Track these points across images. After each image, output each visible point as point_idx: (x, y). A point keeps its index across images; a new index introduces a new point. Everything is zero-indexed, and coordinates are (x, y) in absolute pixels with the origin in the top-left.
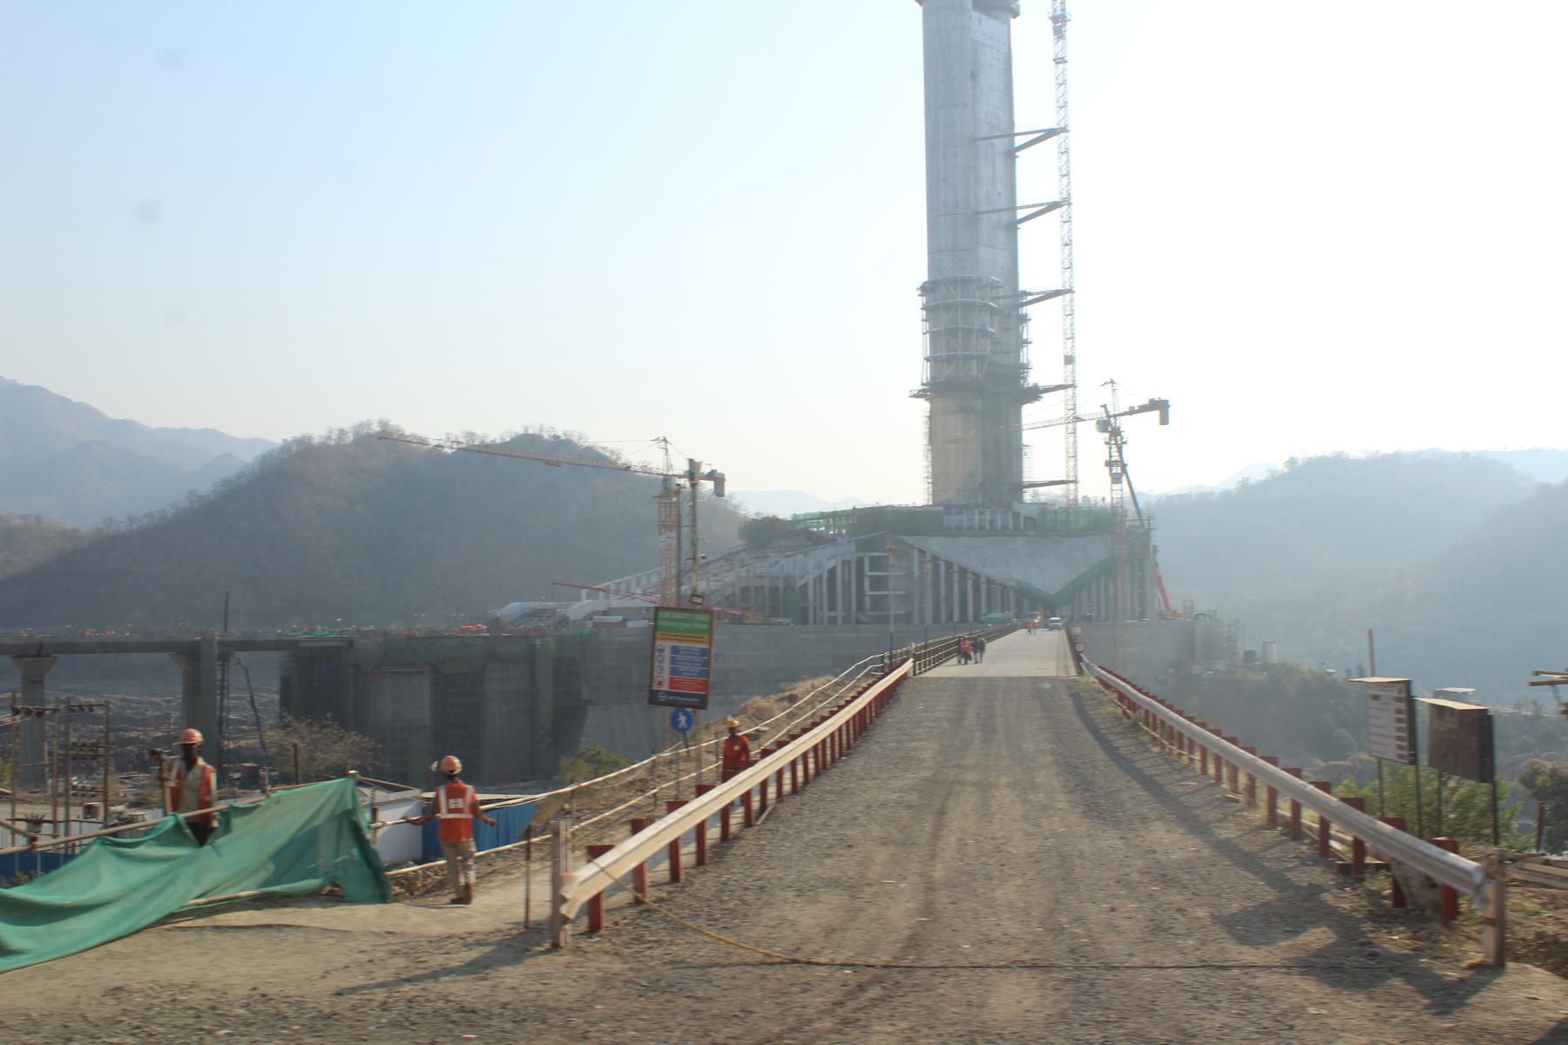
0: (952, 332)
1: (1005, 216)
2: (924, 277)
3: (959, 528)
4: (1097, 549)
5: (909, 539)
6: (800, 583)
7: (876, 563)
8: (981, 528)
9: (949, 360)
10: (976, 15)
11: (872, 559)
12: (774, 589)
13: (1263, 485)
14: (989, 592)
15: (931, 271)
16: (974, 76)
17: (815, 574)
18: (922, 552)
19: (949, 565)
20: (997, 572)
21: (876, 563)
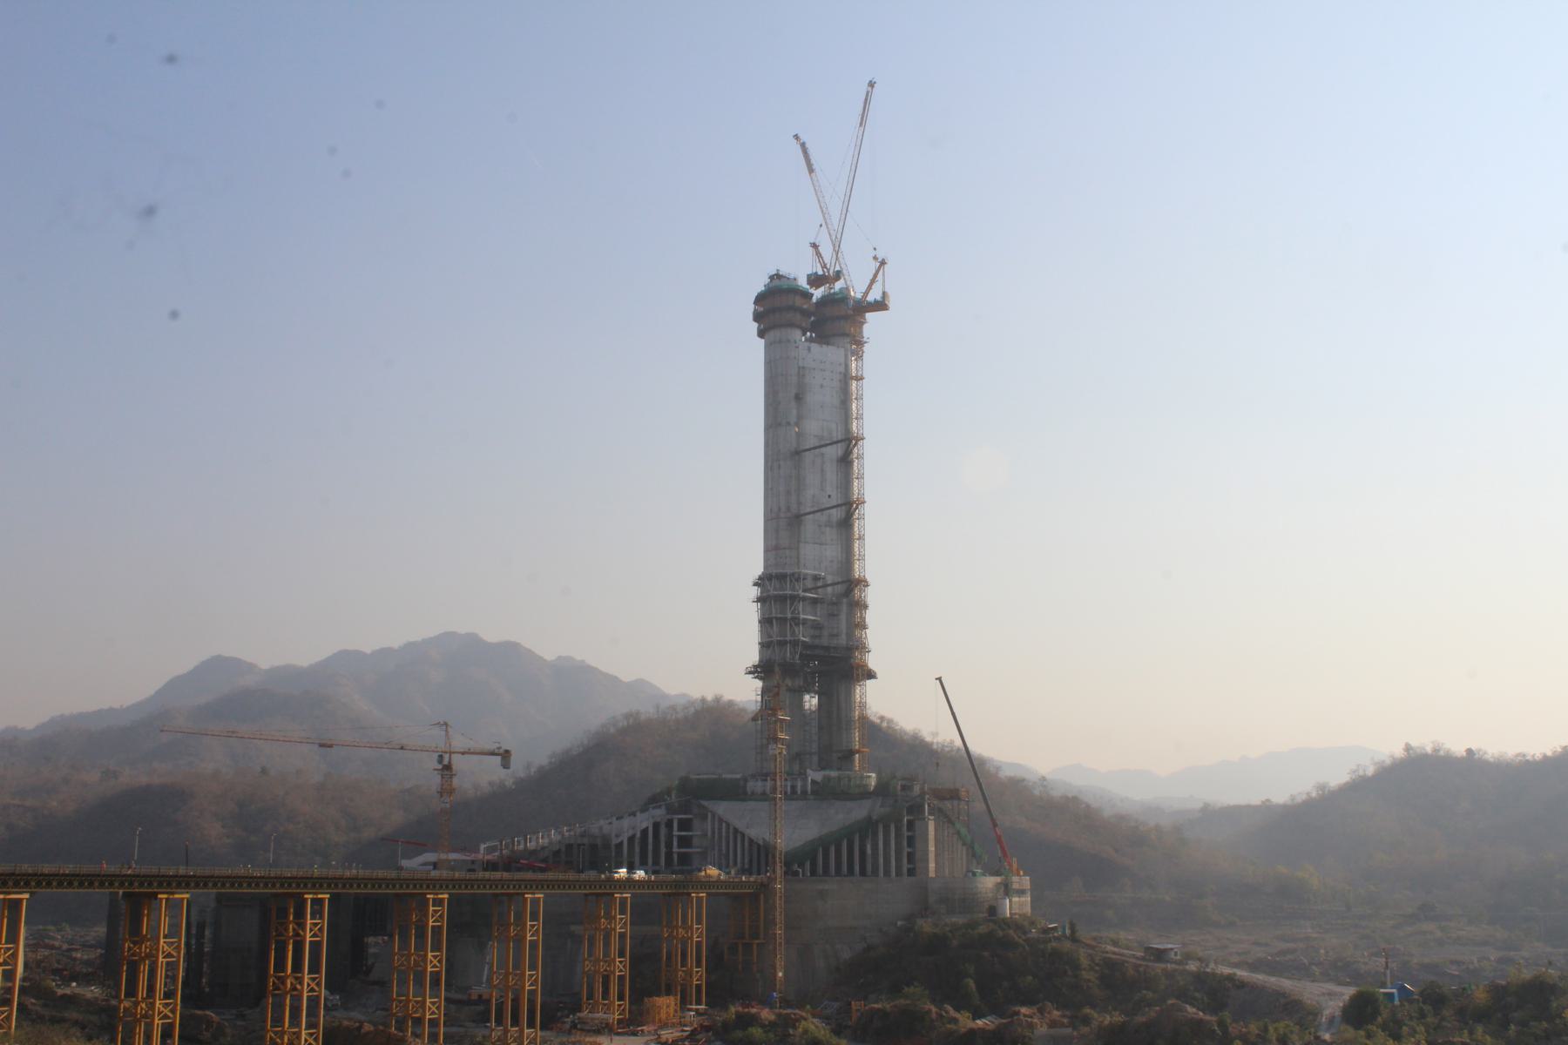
1: (837, 514)
2: (758, 569)
4: (858, 812)
5: (705, 803)
6: (615, 841)
11: (680, 821)
12: (594, 847)
16: (799, 398)
17: (631, 833)
19: (728, 825)
20: (753, 833)
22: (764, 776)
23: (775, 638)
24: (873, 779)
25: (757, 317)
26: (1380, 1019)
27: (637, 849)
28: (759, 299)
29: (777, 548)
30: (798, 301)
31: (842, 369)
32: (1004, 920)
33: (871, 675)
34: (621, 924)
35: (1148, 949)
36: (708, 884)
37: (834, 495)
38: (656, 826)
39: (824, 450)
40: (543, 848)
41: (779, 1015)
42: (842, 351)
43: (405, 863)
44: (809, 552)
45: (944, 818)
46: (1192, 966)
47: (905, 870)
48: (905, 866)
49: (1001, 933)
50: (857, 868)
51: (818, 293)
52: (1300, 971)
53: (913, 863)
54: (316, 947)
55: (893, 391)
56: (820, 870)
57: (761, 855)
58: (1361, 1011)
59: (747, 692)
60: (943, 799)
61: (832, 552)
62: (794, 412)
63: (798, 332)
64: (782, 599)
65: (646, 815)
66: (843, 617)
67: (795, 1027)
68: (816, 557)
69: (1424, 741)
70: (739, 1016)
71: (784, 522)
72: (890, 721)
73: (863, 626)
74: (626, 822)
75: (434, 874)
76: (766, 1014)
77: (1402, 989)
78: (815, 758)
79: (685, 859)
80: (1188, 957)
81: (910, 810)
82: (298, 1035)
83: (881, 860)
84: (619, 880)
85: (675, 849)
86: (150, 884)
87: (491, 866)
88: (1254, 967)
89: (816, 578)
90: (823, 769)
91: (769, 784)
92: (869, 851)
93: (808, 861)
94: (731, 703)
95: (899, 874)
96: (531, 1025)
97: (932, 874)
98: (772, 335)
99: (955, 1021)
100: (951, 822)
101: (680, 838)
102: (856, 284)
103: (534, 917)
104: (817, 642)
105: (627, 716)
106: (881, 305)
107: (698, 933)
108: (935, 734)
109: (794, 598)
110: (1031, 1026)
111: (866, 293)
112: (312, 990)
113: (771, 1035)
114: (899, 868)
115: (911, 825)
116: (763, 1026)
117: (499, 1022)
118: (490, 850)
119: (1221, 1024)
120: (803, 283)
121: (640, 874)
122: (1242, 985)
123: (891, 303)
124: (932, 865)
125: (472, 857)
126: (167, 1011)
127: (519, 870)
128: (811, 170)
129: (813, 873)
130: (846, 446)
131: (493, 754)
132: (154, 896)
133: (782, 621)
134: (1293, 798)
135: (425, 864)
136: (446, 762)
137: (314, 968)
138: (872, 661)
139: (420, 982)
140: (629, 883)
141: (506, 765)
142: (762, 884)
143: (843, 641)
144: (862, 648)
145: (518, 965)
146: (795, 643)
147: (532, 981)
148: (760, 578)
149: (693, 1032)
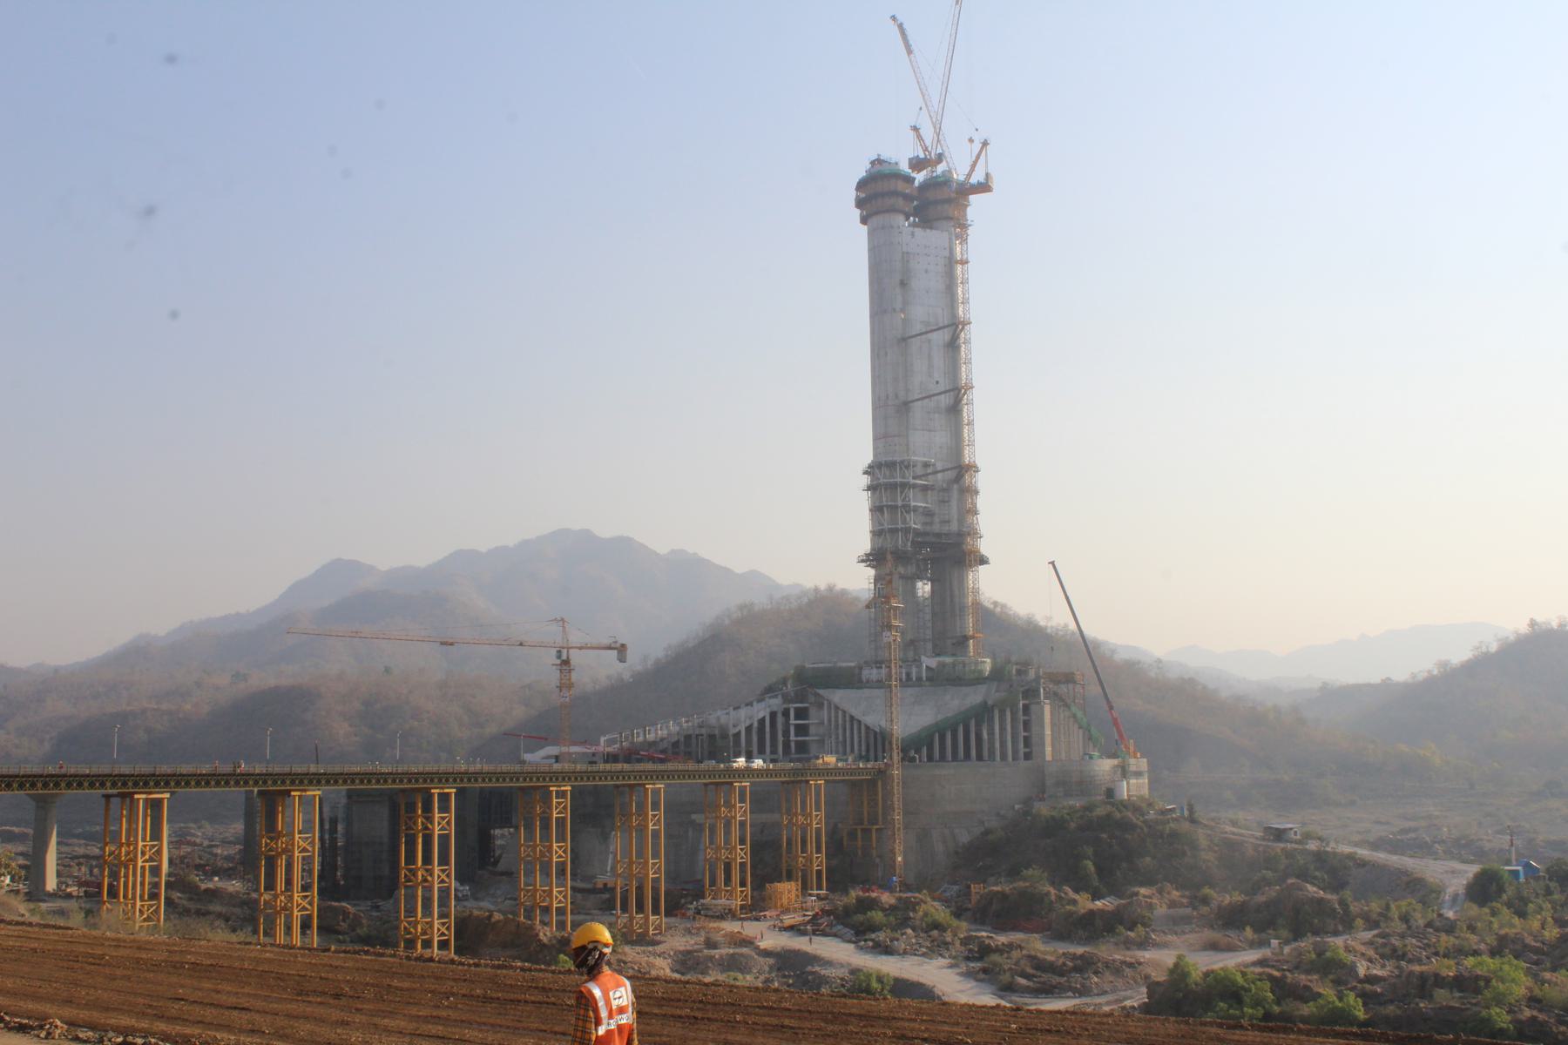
1: (945, 400)
2: (868, 458)
4: (974, 697)
5: (821, 692)
6: (733, 731)
12: (712, 737)
14: (867, 737)
15: (875, 455)
16: (903, 284)
21: (802, 713)
22: (878, 664)
23: (886, 526)
24: (987, 665)
25: (860, 204)
26: (1505, 897)
27: (755, 738)
28: (861, 185)
30: (901, 186)
31: (947, 253)
32: (1122, 802)
33: (983, 561)
34: (741, 812)
35: (1268, 829)
36: (826, 771)
37: (941, 381)
38: (773, 715)
40: (662, 740)
41: (899, 899)
42: (945, 234)
43: (527, 757)
45: (1059, 700)
46: (1312, 846)
47: (1021, 755)
49: (1118, 815)
50: (973, 753)
51: (920, 177)
52: (1423, 849)
53: (1029, 746)
54: (444, 839)
57: (877, 742)
58: (1485, 889)
59: (860, 581)
60: (1059, 682)
61: (941, 438)
63: (901, 218)
64: (892, 487)
65: (762, 705)
66: (954, 503)
67: (914, 910)
68: (925, 445)
70: (859, 900)
71: (893, 409)
72: (1004, 606)
73: (976, 513)
74: (743, 712)
75: (557, 767)
76: (887, 898)
77: (1527, 866)
78: (929, 646)
79: (802, 747)
80: (1308, 836)
81: (1026, 694)
82: (431, 925)
83: (997, 745)
84: (737, 770)
85: (792, 738)
86: (283, 782)
87: (612, 758)
88: (1375, 846)
89: (926, 465)
90: (938, 655)
91: (884, 671)
92: (985, 736)
93: (923, 747)
94: (844, 592)
96: (656, 911)
97: (1049, 757)
98: (875, 220)
99: (1074, 902)
100: (1067, 706)
101: (797, 726)
102: (958, 166)
103: (656, 806)
104: (928, 528)
105: (741, 608)
106: (984, 187)
107: (817, 820)
108: (1049, 619)
109: (904, 486)
110: (1150, 907)
111: (969, 175)
112: (442, 881)
113: (892, 919)
114: (1015, 752)
115: (1026, 709)
116: (883, 910)
117: (625, 908)
118: (610, 742)
119: (1342, 902)
120: (904, 167)
121: (758, 763)
122: (1362, 864)
123: (994, 185)
124: (1048, 749)
125: (593, 750)
126: (305, 904)
127: (639, 761)
128: (910, 52)
129: (930, 759)
130: (954, 329)
131: (610, 648)
132: (288, 793)
133: (893, 508)
134: (1414, 676)
135: (548, 757)
137: (444, 860)
138: (984, 547)
139: (546, 871)
140: (747, 772)
141: (622, 659)
142: (880, 771)
143: (954, 527)
144: (974, 533)
145: (640, 853)
146: (907, 531)
147: (655, 869)
148: (870, 467)
149: (815, 916)
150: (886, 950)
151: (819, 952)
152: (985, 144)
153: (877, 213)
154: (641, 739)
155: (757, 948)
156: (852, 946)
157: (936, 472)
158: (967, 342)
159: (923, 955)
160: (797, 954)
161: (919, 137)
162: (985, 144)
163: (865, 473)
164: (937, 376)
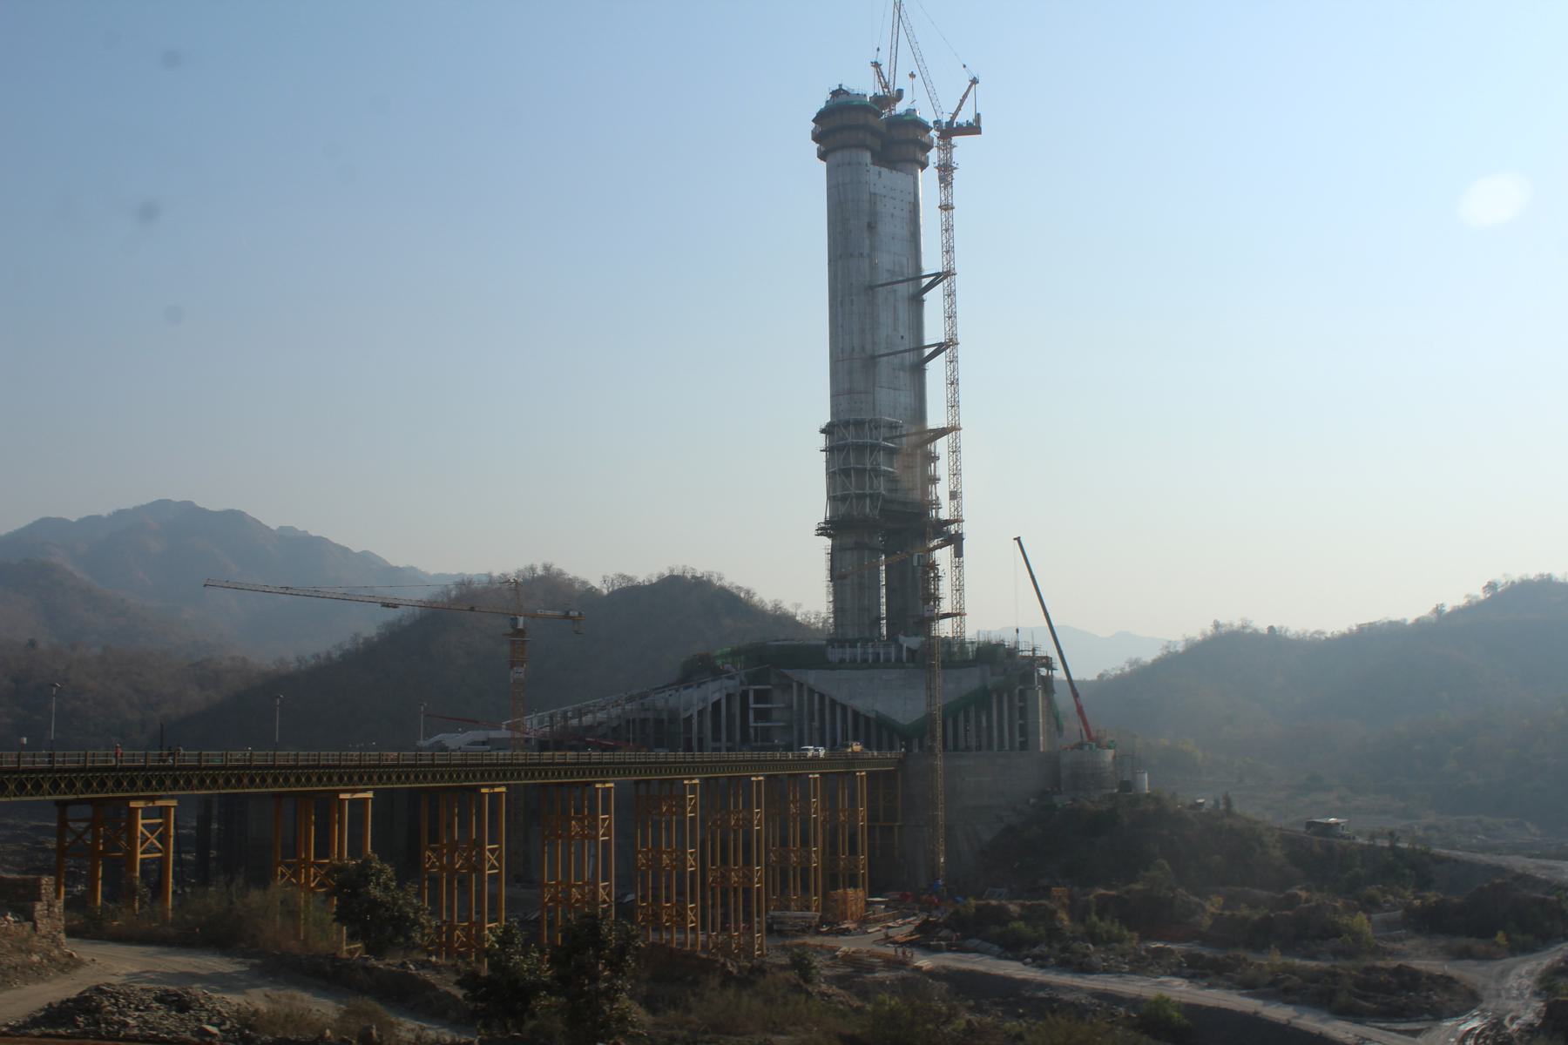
0: (846, 472)
1: (909, 358)
2: (826, 418)
3: (842, 661)
4: (971, 681)
7: (762, 696)
8: (865, 661)
9: (844, 499)
10: (874, 169)
11: (756, 691)
13: (1458, 612)
16: (871, 227)
18: (801, 685)
19: (822, 697)
20: (860, 704)
21: (762, 696)
23: (853, 490)
27: (708, 723)
28: (819, 118)
29: (850, 392)
30: (871, 119)
35: (1310, 825)
36: (854, 759)
38: (729, 697)
39: (899, 287)
40: (600, 724)
44: (884, 397)
48: (1018, 739)
55: (971, 222)
56: (950, 744)
57: (875, 730)
61: (905, 398)
62: (867, 242)
64: (860, 449)
68: (888, 403)
69: (1232, 617)
72: (748, 592)
83: (995, 734)
84: (811, 759)
85: (752, 724)
87: (543, 746)
89: (893, 426)
91: (859, 651)
94: (560, 573)
95: (1012, 748)
106: (973, 129)
108: (798, 606)
109: (874, 448)
111: (956, 114)
115: (1022, 692)
133: (861, 472)
135: (474, 743)
136: (521, 626)
150: (1085, 969)
151: (1001, 972)
152: (974, 81)
153: (843, 147)
154: (575, 722)
155: (919, 969)
156: (1019, 964)
157: (901, 436)
158: (950, 294)
159: (1131, 972)
160: (972, 974)
161: (880, 74)
162: (974, 81)
163: (823, 431)
164: (902, 331)
